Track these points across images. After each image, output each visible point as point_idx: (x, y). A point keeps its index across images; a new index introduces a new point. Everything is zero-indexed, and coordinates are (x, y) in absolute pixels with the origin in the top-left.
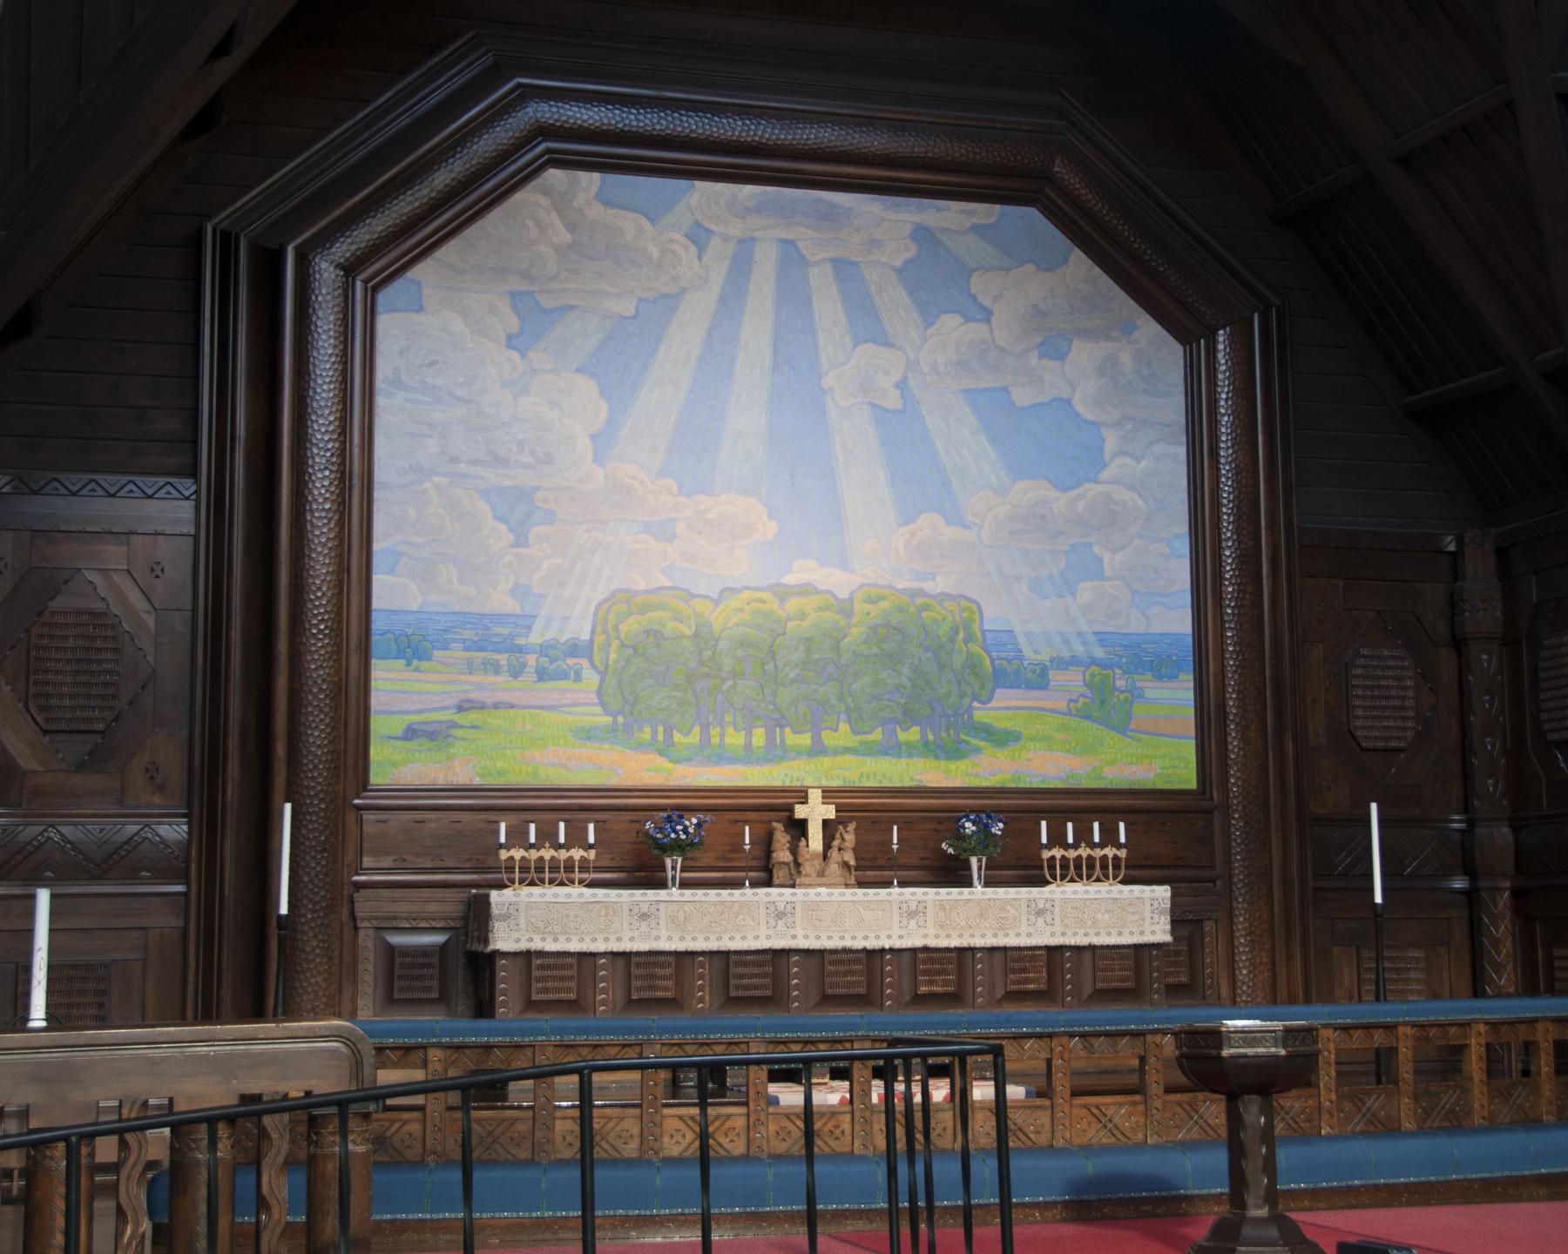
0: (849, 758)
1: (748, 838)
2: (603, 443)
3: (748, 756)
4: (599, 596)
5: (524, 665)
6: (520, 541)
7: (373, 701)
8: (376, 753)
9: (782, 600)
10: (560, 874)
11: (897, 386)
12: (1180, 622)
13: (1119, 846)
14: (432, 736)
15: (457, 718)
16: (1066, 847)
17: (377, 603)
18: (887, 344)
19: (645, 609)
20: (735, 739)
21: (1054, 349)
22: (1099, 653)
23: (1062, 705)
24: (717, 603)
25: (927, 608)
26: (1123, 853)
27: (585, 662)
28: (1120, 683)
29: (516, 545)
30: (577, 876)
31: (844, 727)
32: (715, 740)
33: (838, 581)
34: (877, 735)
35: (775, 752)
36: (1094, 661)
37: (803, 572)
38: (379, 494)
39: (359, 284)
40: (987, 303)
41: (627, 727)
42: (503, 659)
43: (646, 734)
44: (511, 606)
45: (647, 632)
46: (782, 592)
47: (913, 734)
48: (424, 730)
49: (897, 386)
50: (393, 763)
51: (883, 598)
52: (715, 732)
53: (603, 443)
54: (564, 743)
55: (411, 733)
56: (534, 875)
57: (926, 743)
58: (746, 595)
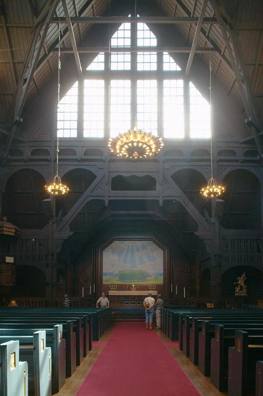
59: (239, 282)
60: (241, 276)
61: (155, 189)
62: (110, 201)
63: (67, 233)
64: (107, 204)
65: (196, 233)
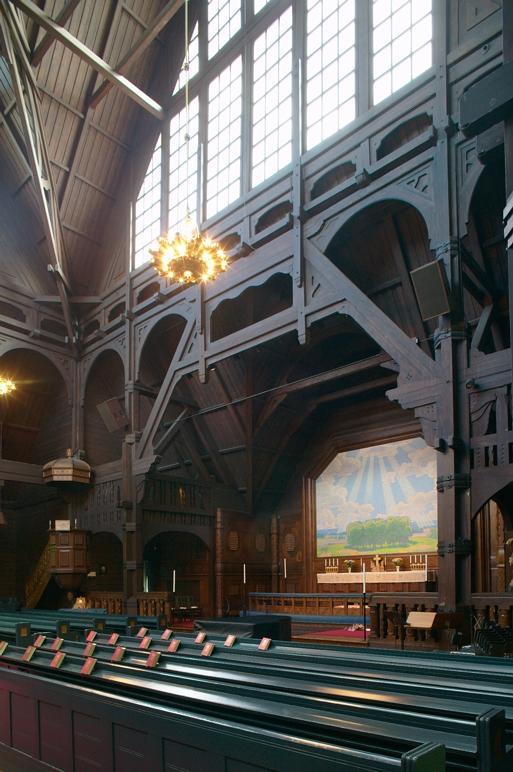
3: (370, 550)
6: (336, 516)
33: (384, 517)
37: (379, 516)
46: (375, 520)
47: (397, 544)
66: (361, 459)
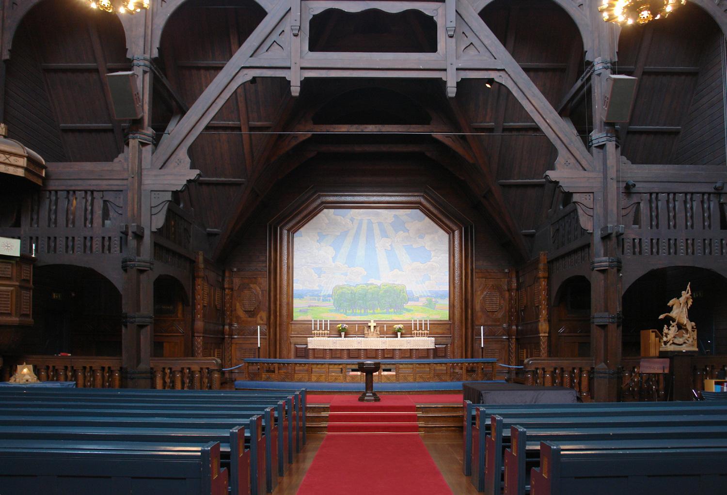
0: (380, 315)
1: (362, 329)
2: (334, 259)
3: (361, 315)
4: (334, 286)
5: (320, 299)
6: (319, 277)
7: (294, 305)
8: (294, 315)
9: (367, 286)
10: (323, 335)
11: (390, 245)
12: (446, 288)
13: (427, 330)
14: (304, 311)
15: (309, 308)
16: (417, 331)
17: (294, 289)
18: (389, 238)
19: (342, 288)
20: (358, 311)
21: (422, 237)
22: (429, 294)
23: (422, 304)
24: (355, 287)
25: (396, 287)
26: (428, 332)
27: (331, 298)
28: (433, 300)
29: (319, 277)
30: (326, 335)
31: (379, 309)
32: (355, 312)
33: (378, 283)
34: (385, 311)
35: (366, 314)
36: (428, 296)
37: (371, 281)
38: (294, 269)
39: (290, 233)
40: (408, 229)
41: (338, 310)
42: (316, 298)
43: (342, 311)
44: (318, 289)
45: (342, 293)
46: (367, 285)
48: (303, 309)
49: (390, 245)
50: (297, 316)
51: (386, 285)
52: (355, 310)
53: (334, 259)
54: (326, 313)
55: (301, 311)
56: (319, 335)
57: (395, 312)
58: (361, 285)
59: (673, 314)
60: (679, 296)
61: (433, 48)
62: (307, 83)
63: (181, 173)
64: (295, 91)
65: (552, 175)
66: (352, 220)
